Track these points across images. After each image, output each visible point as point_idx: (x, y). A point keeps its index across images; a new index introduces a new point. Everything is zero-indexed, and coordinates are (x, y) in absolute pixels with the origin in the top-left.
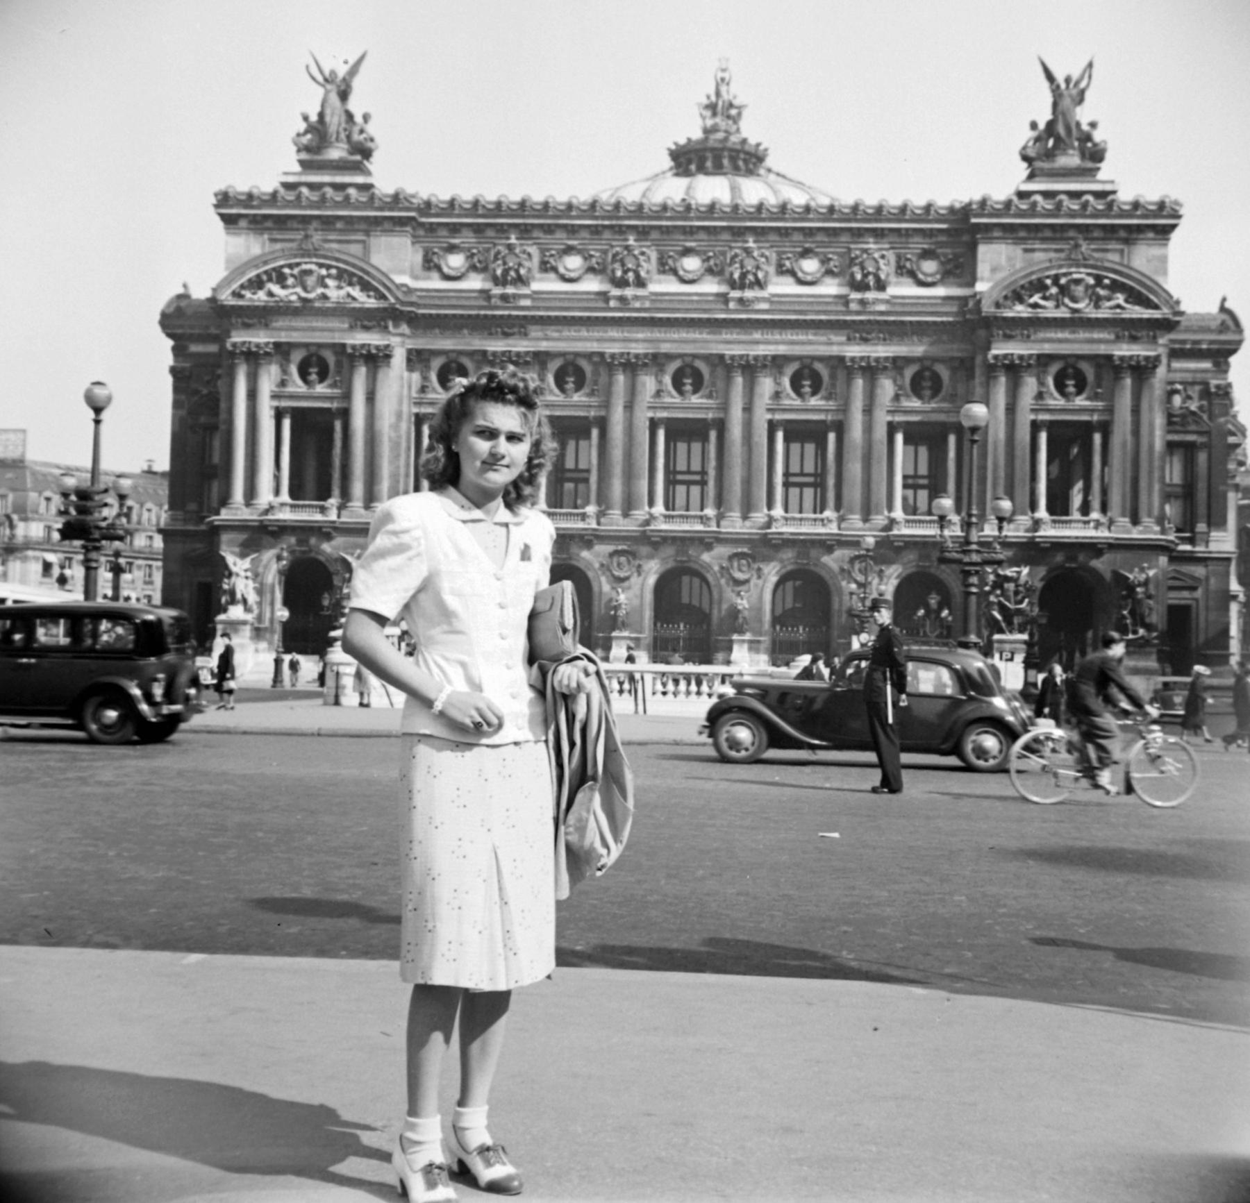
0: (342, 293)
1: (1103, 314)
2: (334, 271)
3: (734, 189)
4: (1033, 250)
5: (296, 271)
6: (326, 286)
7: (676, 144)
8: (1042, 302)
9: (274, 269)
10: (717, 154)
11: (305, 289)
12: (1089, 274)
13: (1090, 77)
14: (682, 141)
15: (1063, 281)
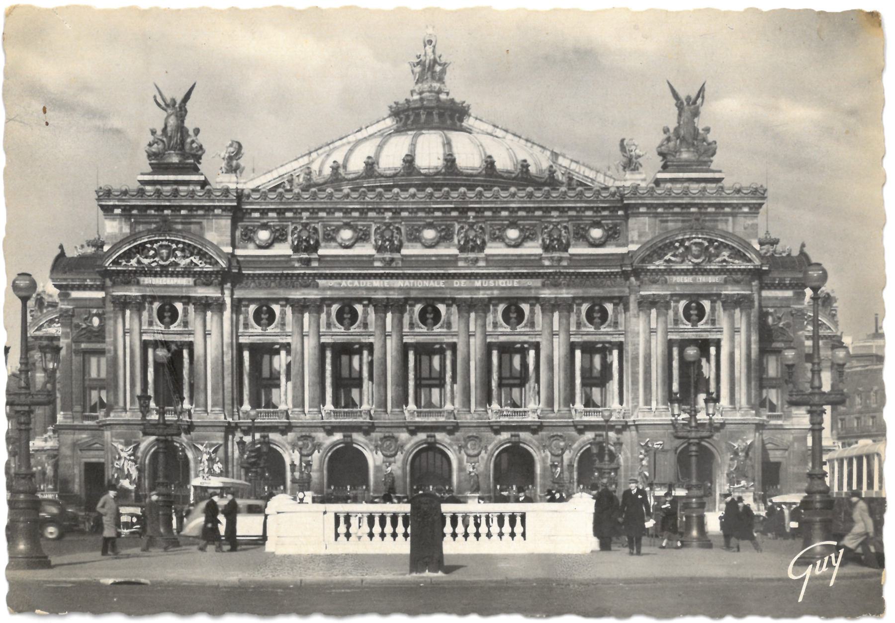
0: (188, 260)
1: (713, 267)
2: (181, 246)
3: (448, 144)
4: (667, 221)
5: (155, 246)
6: (176, 257)
7: (396, 103)
8: (673, 259)
9: (140, 244)
10: (429, 111)
11: (162, 258)
12: (705, 239)
13: (703, 97)
14: (402, 101)
15: (687, 244)
